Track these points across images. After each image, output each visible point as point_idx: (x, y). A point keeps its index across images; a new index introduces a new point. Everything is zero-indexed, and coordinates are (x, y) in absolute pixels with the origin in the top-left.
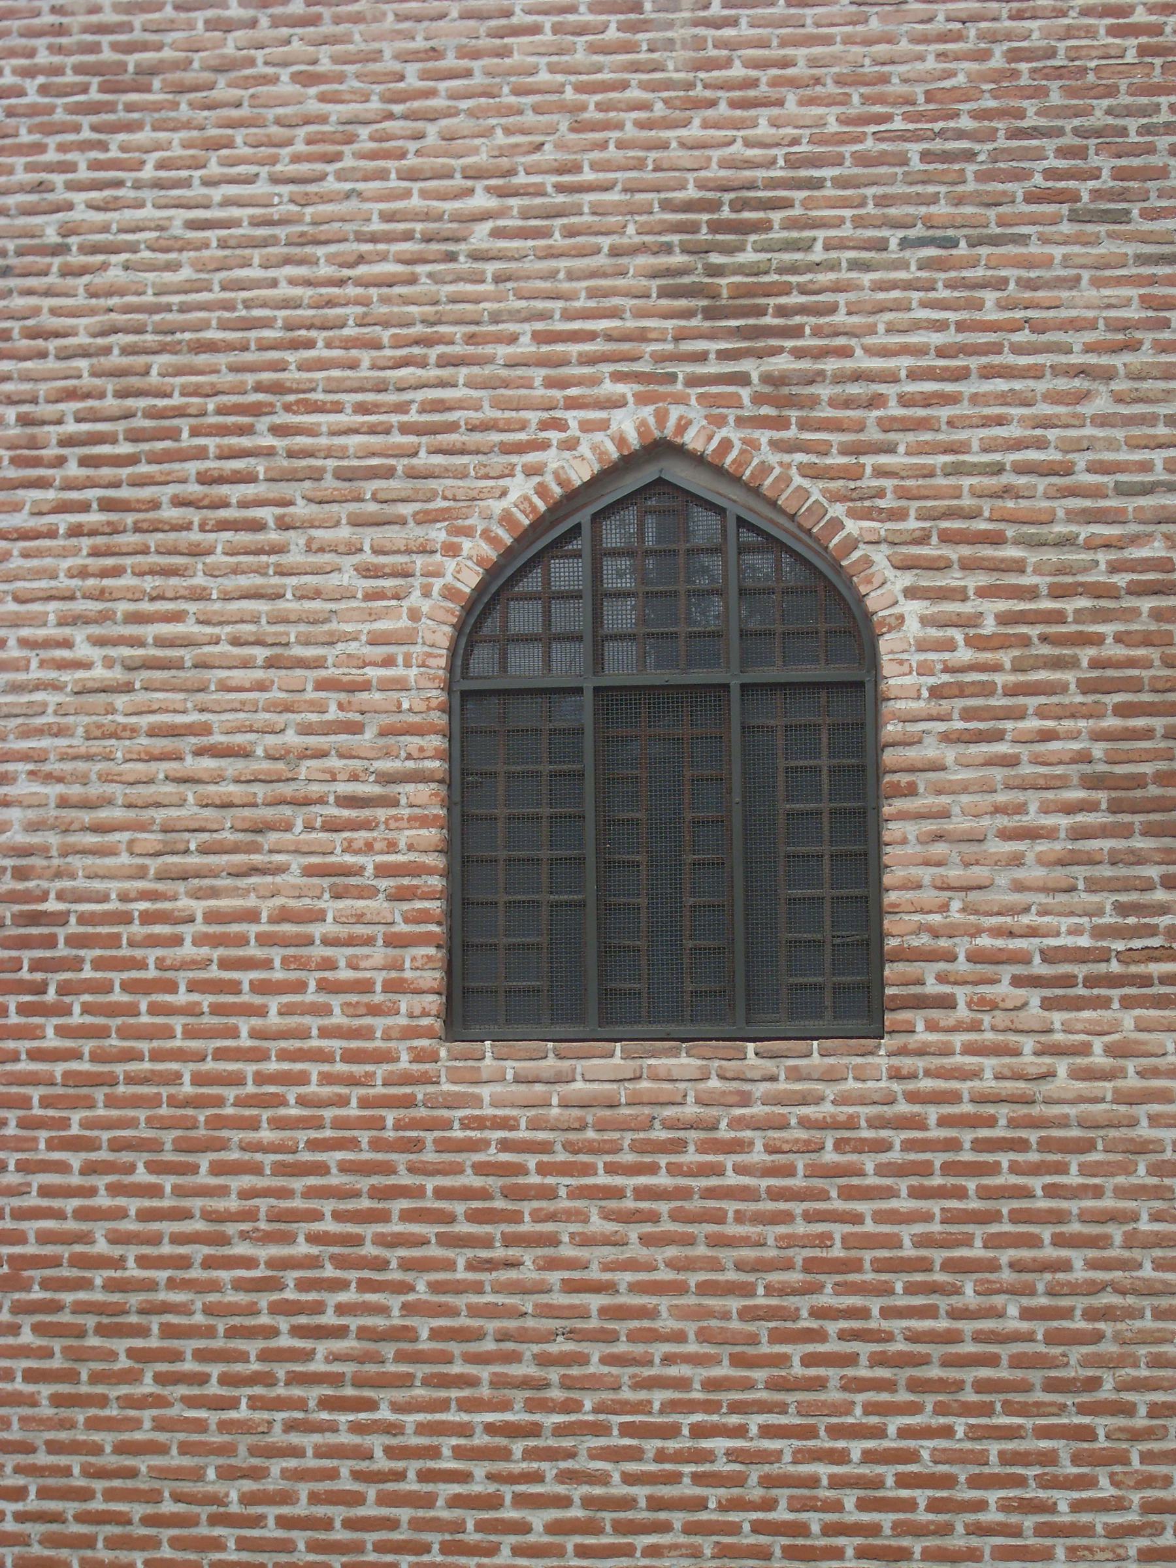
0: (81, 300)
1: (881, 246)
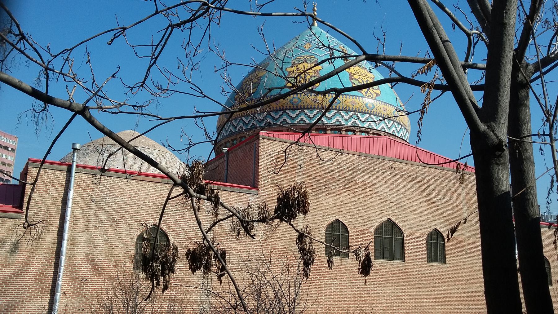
0: (107, 207)
1: (173, 210)
